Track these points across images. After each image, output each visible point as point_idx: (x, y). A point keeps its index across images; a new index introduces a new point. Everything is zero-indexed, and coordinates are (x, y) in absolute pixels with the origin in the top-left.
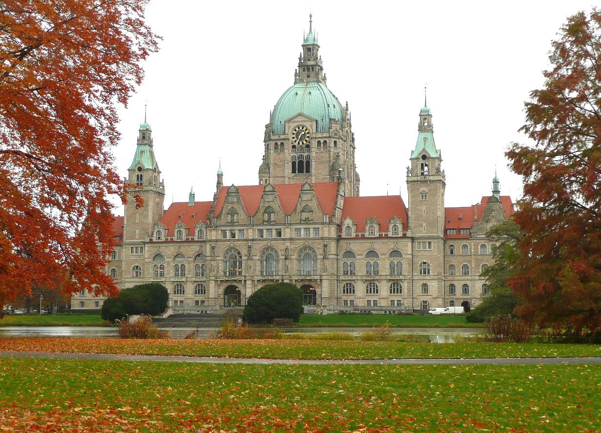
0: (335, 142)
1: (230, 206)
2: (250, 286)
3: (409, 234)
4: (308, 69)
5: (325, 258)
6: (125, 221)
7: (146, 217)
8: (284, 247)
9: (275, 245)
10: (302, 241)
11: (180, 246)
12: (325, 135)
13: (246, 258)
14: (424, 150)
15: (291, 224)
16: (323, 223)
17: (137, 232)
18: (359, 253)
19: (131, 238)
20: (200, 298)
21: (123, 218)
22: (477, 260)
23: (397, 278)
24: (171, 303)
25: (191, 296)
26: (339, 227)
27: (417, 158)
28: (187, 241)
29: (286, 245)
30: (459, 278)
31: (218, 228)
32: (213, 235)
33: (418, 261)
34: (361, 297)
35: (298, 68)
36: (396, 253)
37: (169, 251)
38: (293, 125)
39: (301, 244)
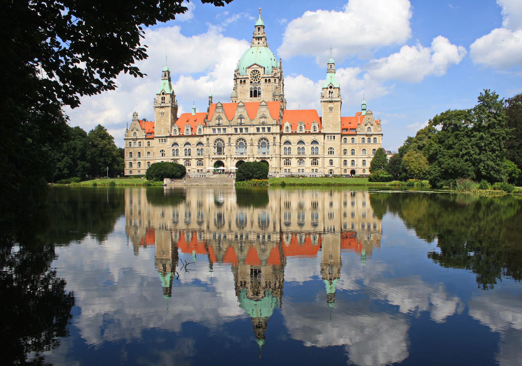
0: (275, 80)
1: (217, 115)
4: (259, 40)
5: (274, 145)
6: (155, 125)
7: (167, 121)
15: (254, 125)
16: (273, 125)
19: (159, 134)
20: (200, 168)
22: (360, 146)
23: (316, 156)
24: (187, 172)
26: (281, 128)
27: (327, 88)
32: (208, 131)
33: (327, 147)
34: (294, 167)
36: (315, 142)
37: (181, 141)
38: (251, 70)
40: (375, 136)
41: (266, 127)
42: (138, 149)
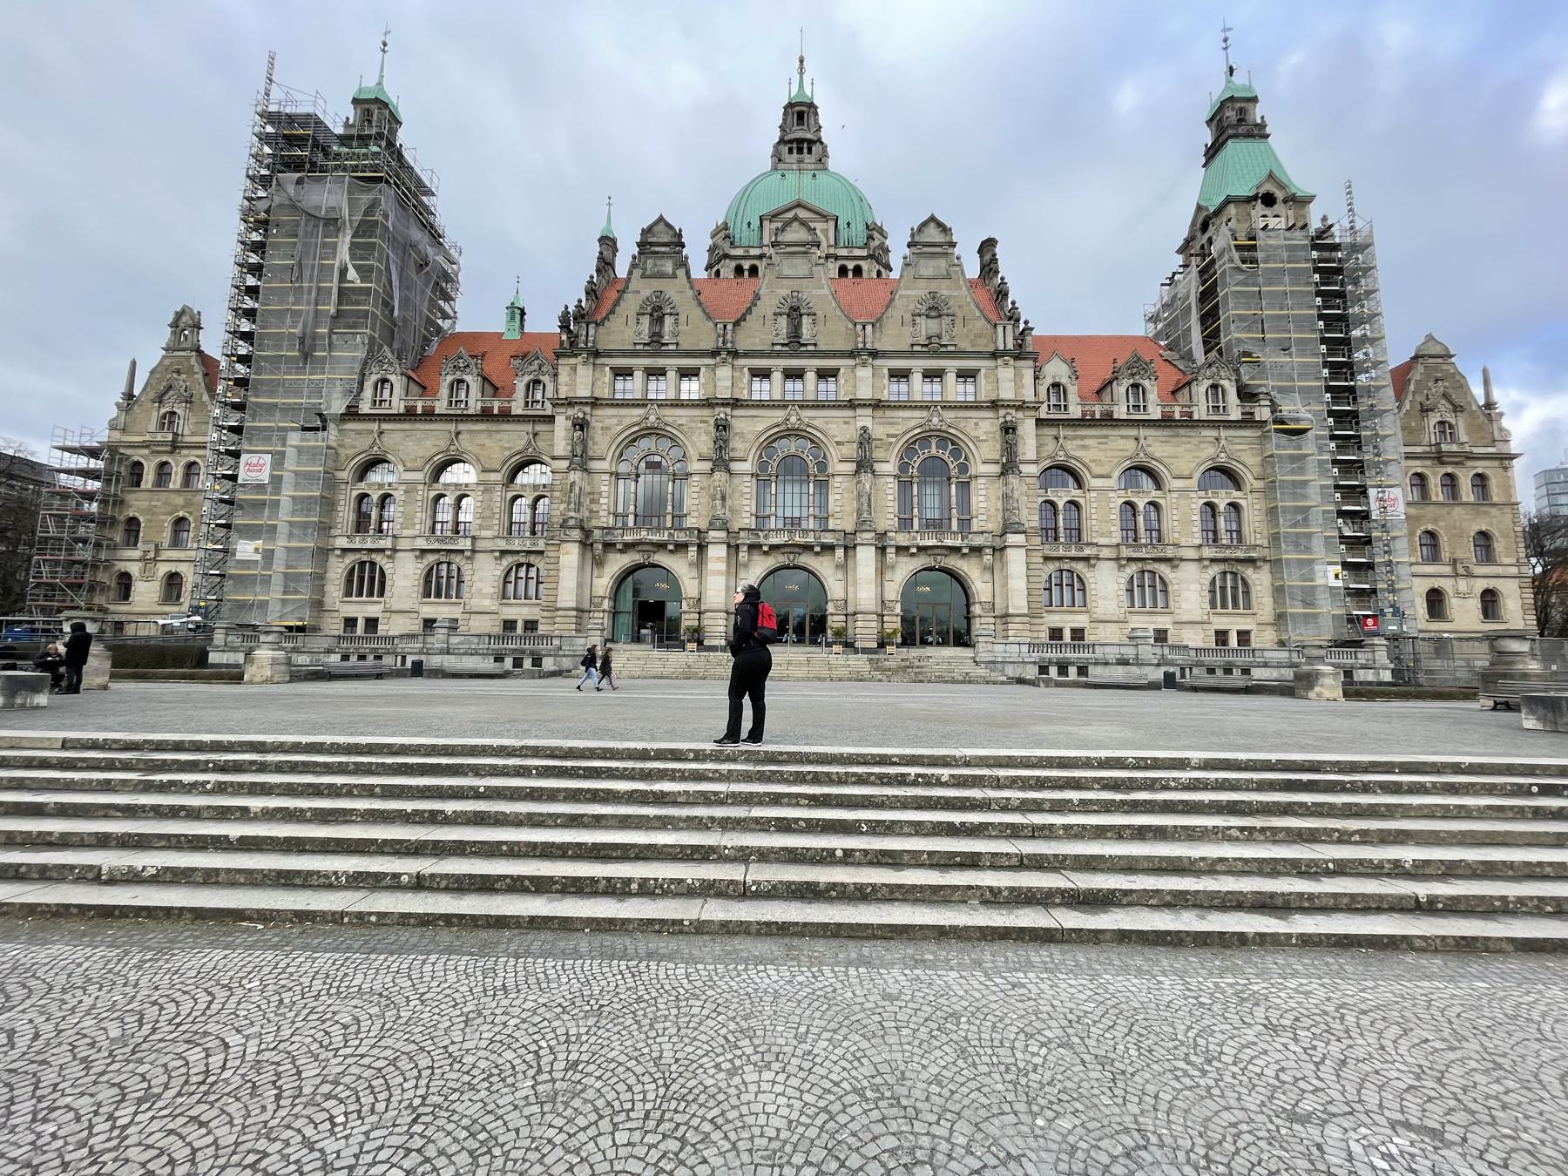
2: (723, 566)
3: (1263, 413)
4: (800, 151)
8: (851, 432)
9: (815, 423)
10: (917, 414)
11: (458, 434)
12: (857, 252)
13: (707, 466)
14: (1271, 176)
15: (875, 354)
16: (995, 355)
18: (1097, 470)
25: (487, 604)
28: (486, 415)
29: (860, 424)
31: (599, 361)
39: (914, 423)
40: (1480, 467)
41: (952, 365)
42: (179, 500)
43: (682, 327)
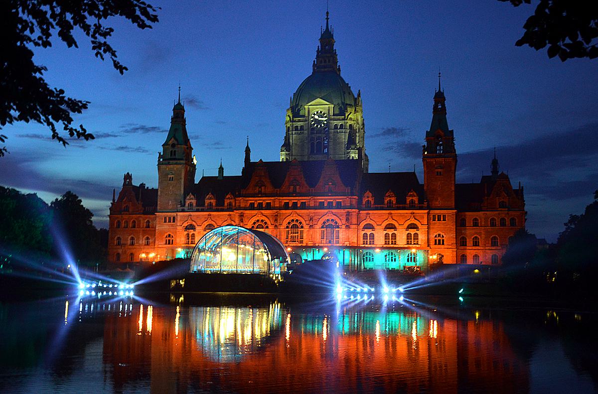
6: (159, 193)
17: (170, 203)
21: (157, 190)
30: (470, 248)
35: (316, 60)
43: (266, 190)
